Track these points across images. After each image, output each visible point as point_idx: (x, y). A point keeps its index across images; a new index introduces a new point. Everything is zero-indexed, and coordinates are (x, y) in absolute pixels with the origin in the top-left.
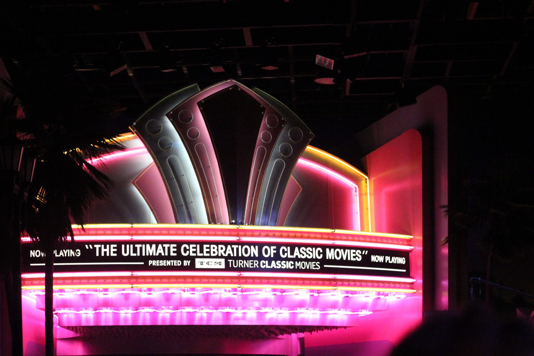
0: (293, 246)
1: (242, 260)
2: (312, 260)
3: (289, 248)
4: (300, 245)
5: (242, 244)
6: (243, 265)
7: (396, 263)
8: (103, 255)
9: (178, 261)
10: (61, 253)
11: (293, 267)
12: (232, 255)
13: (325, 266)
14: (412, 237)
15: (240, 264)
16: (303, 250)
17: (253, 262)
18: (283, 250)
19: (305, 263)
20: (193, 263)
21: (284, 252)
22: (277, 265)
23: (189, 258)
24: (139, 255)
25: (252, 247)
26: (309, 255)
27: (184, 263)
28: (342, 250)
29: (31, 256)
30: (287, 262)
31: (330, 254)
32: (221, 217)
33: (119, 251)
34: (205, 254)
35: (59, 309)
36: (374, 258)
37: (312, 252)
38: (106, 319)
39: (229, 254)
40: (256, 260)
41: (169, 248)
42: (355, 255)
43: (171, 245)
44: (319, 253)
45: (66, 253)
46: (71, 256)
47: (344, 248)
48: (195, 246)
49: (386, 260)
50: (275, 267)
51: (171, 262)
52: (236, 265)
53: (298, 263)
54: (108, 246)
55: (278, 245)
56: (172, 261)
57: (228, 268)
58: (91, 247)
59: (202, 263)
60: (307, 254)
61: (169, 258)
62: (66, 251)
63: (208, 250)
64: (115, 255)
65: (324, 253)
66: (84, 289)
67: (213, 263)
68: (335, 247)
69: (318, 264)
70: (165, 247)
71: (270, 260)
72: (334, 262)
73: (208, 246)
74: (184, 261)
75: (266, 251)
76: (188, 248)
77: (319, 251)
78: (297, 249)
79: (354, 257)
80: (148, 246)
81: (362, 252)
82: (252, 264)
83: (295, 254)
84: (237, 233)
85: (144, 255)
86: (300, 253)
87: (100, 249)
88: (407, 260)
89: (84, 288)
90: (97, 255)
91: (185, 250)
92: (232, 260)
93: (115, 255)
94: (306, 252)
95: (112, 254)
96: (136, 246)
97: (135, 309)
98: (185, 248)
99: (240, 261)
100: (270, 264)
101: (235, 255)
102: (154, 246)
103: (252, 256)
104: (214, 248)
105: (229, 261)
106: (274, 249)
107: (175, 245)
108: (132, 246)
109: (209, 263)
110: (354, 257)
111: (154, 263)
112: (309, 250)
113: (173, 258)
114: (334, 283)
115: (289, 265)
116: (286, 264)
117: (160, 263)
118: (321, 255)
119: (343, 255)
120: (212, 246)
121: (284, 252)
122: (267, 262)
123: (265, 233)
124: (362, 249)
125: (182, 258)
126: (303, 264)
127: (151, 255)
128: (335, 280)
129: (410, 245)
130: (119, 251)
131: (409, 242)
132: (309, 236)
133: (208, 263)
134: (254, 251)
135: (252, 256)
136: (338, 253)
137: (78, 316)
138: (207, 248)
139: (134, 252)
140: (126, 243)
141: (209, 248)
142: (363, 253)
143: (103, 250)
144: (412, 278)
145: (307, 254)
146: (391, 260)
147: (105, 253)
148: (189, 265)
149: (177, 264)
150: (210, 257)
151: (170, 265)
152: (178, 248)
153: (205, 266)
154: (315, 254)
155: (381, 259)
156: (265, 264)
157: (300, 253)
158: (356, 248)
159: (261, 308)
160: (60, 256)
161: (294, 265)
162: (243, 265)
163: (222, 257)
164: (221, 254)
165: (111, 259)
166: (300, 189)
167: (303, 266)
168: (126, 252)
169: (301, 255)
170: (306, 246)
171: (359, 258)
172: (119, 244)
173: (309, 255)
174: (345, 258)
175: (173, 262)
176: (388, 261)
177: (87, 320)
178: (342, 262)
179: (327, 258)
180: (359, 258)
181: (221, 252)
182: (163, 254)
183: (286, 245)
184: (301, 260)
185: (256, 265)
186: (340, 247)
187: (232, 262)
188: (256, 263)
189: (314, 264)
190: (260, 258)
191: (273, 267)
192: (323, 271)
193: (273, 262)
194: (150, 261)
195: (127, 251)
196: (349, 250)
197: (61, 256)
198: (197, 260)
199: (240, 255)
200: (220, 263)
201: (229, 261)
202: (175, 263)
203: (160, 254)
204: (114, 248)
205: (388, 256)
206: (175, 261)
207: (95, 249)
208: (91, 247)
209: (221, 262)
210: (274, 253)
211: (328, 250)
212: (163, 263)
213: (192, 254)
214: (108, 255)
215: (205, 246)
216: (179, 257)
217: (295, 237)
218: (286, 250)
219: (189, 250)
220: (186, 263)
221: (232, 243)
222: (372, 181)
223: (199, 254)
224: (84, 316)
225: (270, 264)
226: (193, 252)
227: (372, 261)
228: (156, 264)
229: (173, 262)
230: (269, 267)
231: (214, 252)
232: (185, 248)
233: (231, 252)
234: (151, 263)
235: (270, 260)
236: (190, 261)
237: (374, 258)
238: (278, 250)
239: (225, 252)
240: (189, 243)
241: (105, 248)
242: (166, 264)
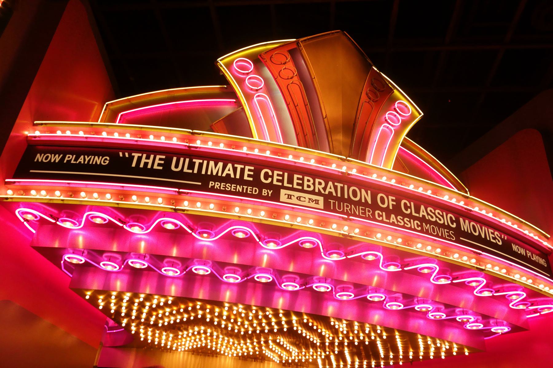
3: (412, 204)
6: (351, 210)
8: (142, 166)
10: (81, 159)
12: (334, 194)
15: (345, 208)
16: (431, 211)
17: (365, 210)
18: (405, 204)
21: (406, 207)
22: (398, 221)
23: (270, 186)
24: (196, 171)
25: (363, 191)
26: (440, 220)
27: (263, 192)
29: (36, 160)
31: (466, 225)
33: (167, 163)
34: (295, 186)
36: (515, 248)
37: (443, 216)
39: (330, 193)
41: (243, 170)
43: (246, 167)
45: (87, 159)
46: (94, 163)
49: (528, 255)
51: (243, 188)
54: (152, 156)
56: (245, 187)
58: (127, 155)
59: (290, 197)
61: (241, 181)
62: (88, 157)
64: (161, 168)
69: (452, 233)
70: (237, 168)
76: (270, 173)
78: (422, 207)
80: (212, 163)
83: (421, 213)
85: (203, 172)
86: (428, 214)
87: (140, 159)
90: (134, 165)
91: (266, 176)
94: (434, 214)
95: (156, 167)
98: (266, 173)
100: (388, 217)
101: (339, 195)
102: (220, 164)
103: (363, 201)
104: (308, 181)
105: (331, 201)
109: (300, 198)
111: (217, 185)
112: (439, 213)
113: (247, 183)
116: (410, 222)
117: (226, 187)
118: (455, 224)
120: (306, 178)
122: (384, 213)
127: (214, 174)
130: (167, 163)
133: (299, 198)
134: (366, 196)
135: (363, 201)
136: (474, 227)
138: (298, 179)
139: (188, 169)
141: (302, 179)
142: (503, 237)
143: (144, 160)
145: (437, 217)
147: (146, 164)
148: (270, 195)
149: (252, 192)
150: (303, 191)
151: (241, 191)
154: (447, 219)
155: (522, 251)
157: (428, 214)
160: (78, 162)
162: (351, 210)
163: (319, 194)
164: (319, 189)
165: (152, 172)
168: (177, 166)
169: (429, 217)
171: (499, 241)
173: (440, 220)
175: (247, 189)
176: (530, 256)
180: (499, 241)
182: (232, 176)
184: (431, 223)
187: (334, 204)
193: (393, 216)
194: (211, 182)
197: (80, 162)
198: (283, 192)
199: (346, 197)
200: (317, 202)
201: (331, 201)
202: (249, 190)
203: (228, 175)
204: (160, 159)
206: (249, 188)
208: (127, 155)
209: (318, 201)
213: (275, 182)
214: (149, 166)
216: (256, 182)
218: (409, 205)
219: (272, 177)
223: (286, 184)
225: (388, 217)
226: (278, 180)
228: (220, 187)
229: (247, 189)
231: (309, 186)
232: (266, 173)
233: (333, 190)
235: (388, 211)
236: (272, 191)
239: (325, 189)
241: (148, 158)
242: (236, 189)
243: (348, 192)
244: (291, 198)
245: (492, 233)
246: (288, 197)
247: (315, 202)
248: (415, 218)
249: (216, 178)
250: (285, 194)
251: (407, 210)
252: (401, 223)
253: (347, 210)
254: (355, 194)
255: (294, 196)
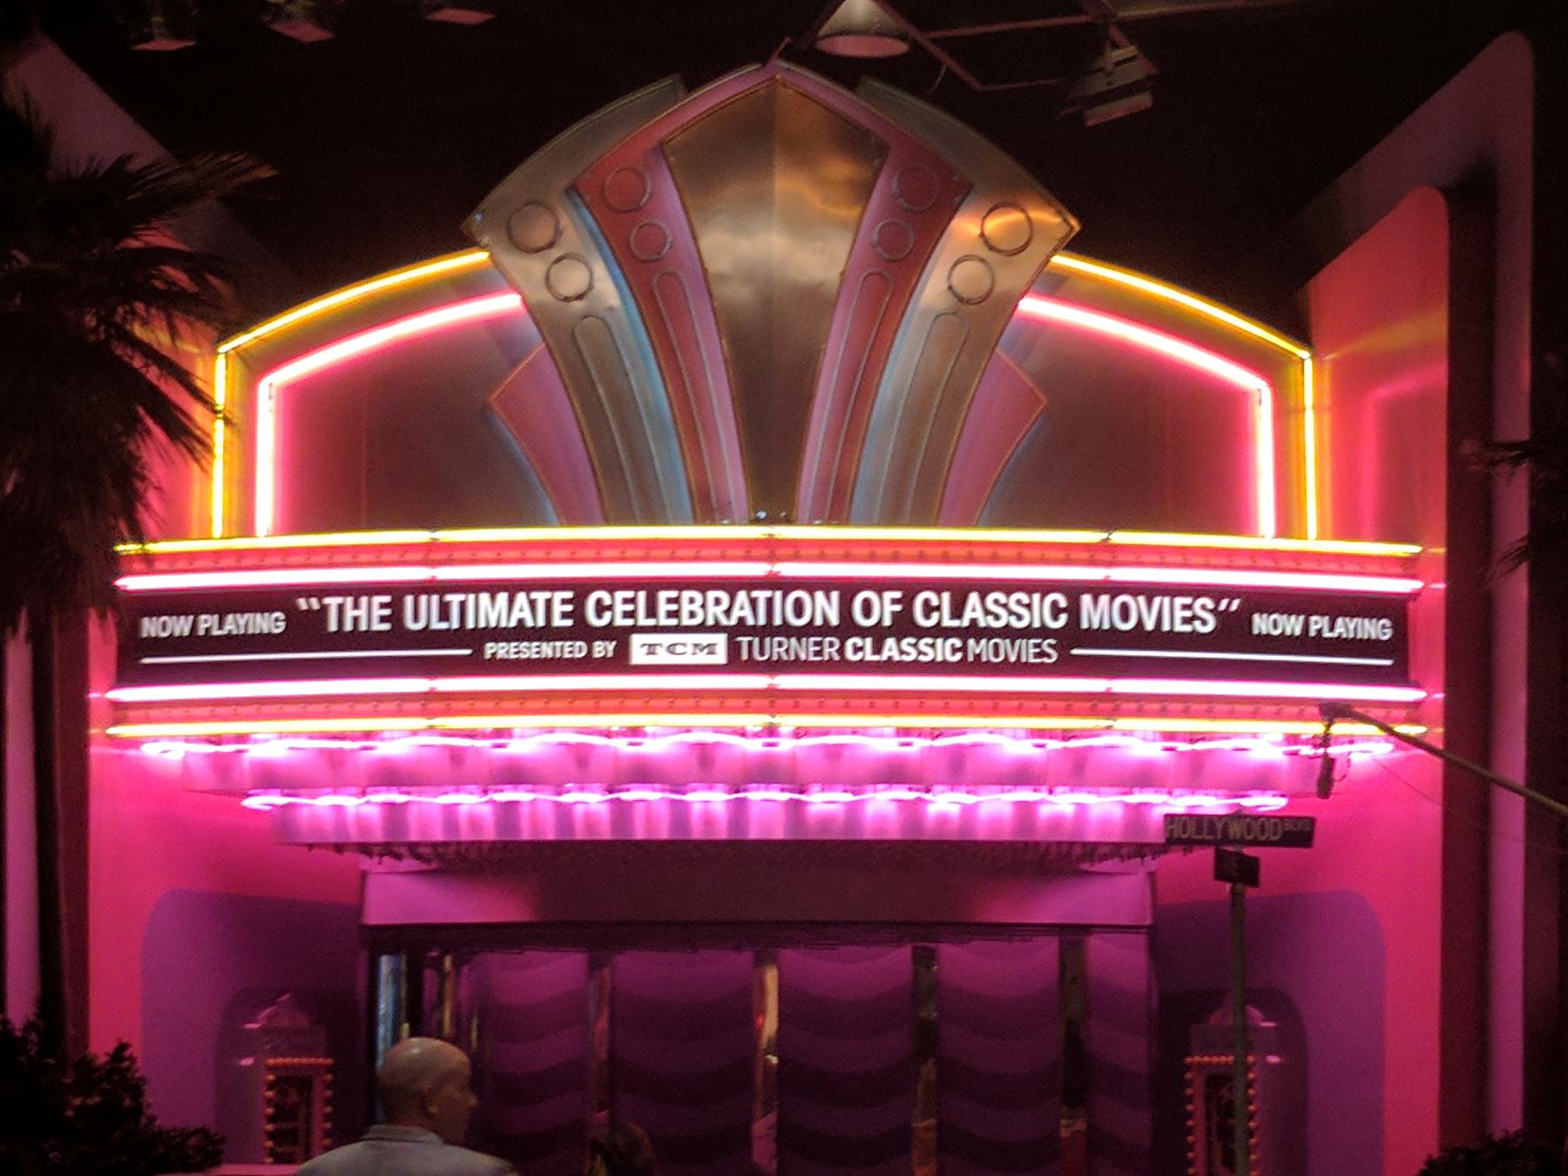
0: (960, 591)
1: (585, 641)
2: (1028, 633)
3: (946, 596)
4: (985, 587)
5: (786, 585)
6: (787, 651)
7: (1351, 636)
8: (348, 627)
9: (578, 643)
11: (959, 656)
13: (1075, 652)
14: (1415, 549)
15: (776, 650)
16: (996, 602)
19: (1004, 644)
20: (623, 650)
21: (928, 609)
22: (902, 652)
23: (609, 632)
24: (455, 625)
25: (819, 595)
26: (1019, 617)
28: (1141, 599)
30: (939, 641)
31: (1095, 613)
32: (730, 503)
33: (396, 617)
34: (664, 621)
35: (498, 787)
36: (1262, 624)
37: (1029, 606)
38: (423, 828)
39: (741, 620)
40: (831, 636)
41: (549, 603)
42: (1188, 614)
44: (1056, 611)
47: (1150, 591)
48: (630, 594)
50: (897, 658)
51: (554, 648)
52: (762, 653)
53: (978, 642)
55: (910, 588)
56: (558, 644)
57: (735, 664)
59: (651, 650)
60: (1011, 613)
61: (547, 633)
63: (674, 607)
64: (386, 627)
65: (1074, 610)
66: (704, 729)
67: (688, 649)
68: (1114, 589)
69: (1050, 645)
71: (878, 635)
72: (1110, 637)
73: (673, 594)
74: (597, 643)
75: (867, 609)
77: (1054, 604)
78: (974, 598)
79: (1186, 621)
81: (1217, 603)
82: (818, 648)
84: (772, 550)
85: (470, 625)
86: (987, 612)
87: (341, 608)
88: (1400, 627)
89: (567, 728)
90: (333, 627)
91: (601, 609)
92: (750, 638)
93: (386, 627)
94: (1005, 606)
96: (448, 597)
97: (731, 790)
99: (777, 639)
100: (877, 650)
102: (502, 597)
106: (894, 601)
107: (569, 595)
108: (435, 598)
110: (1186, 621)
112: (1019, 602)
114: (1109, 706)
115: (944, 650)
116: (933, 646)
118: (1063, 618)
119: (1147, 614)
120: (686, 595)
121: (928, 609)
122: (869, 641)
123: (866, 551)
124: (1217, 592)
125: (588, 634)
126: (996, 645)
128: (1108, 696)
129: (1413, 577)
130: (396, 617)
131: (1407, 567)
132: (1020, 554)
134: (826, 608)
135: (819, 622)
136: (1125, 610)
137: (680, 811)
138: (670, 601)
140: (420, 588)
141: (676, 600)
143: (350, 613)
144: (1417, 686)
145: (1011, 613)
146: (1332, 629)
147: (356, 620)
148: (610, 654)
152: (579, 602)
153: (662, 658)
154: (1040, 612)
155: (1292, 625)
156: (861, 649)
157: (987, 612)
158: (1196, 591)
159: (742, 787)
161: (964, 649)
163: (717, 628)
166: (1040, 401)
167: (996, 654)
168: (416, 618)
169: (990, 618)
170: (1009, 587)
171: (1204, 622)
172: (397, 591)
173: (1019, 617)
174: (1150, 625)
175: (562, 647)
176: (1320, 631)
177: (708, 819)
178: (1138, 637)
179: (1085, 625)
180: (1204, 622)
181: (715, 613)
183: (938, 586)
184: (989, 633)
185: (830, 652)
186: (1135, 589)
187: (750, 644)
188: (831, 644)
189: (1037, 646)
190: (847, 628)
191: (890, 658)
192: (1068, 666)
194: (489, 645)
195: (422, 615)
196: (1167, 600)
198: (637, 640)
199: (778, 621)
200: (711, 648)
205: (1323, 615)
207: (324, 609)
209: (714, 645)
210: (894, 614)
211: (1086, 599)
212: (529, 650)
213: (620, 622)
214: (363, 627)
215: (663, 595)
216: (581, 630)
217: (970, 559)
219: (610, 608)
220: (603, 649)
221: (750, 584)
222: (1327, 367)
223: (643, 621)
224: (697, 809)
225: (877, 650)
226: (627, 615)
227: (1256, 632)
228: (507, 652)
230: (876, 658)
233: (747, 613)
234: (493, 651)
235: (878, 635)
237: (1262, 624)
238: (907, 601)
239: (728, 612)
240: (612, 585)
241: (356, 606)
243: (784, 610)
244: (653, 653)
245: (1186, 607)
246: (649, 649)
247: (706, 651)
248: (945, 633)
249: (499, 634)
250: (644, 645)
251: (927, 616)
252: (908, 654)
253: (779, 653)
254: (799, 609)
255: (660, 645)
